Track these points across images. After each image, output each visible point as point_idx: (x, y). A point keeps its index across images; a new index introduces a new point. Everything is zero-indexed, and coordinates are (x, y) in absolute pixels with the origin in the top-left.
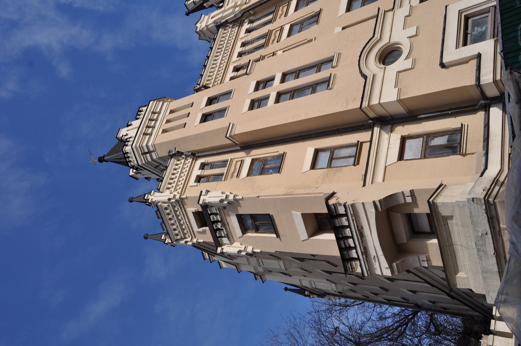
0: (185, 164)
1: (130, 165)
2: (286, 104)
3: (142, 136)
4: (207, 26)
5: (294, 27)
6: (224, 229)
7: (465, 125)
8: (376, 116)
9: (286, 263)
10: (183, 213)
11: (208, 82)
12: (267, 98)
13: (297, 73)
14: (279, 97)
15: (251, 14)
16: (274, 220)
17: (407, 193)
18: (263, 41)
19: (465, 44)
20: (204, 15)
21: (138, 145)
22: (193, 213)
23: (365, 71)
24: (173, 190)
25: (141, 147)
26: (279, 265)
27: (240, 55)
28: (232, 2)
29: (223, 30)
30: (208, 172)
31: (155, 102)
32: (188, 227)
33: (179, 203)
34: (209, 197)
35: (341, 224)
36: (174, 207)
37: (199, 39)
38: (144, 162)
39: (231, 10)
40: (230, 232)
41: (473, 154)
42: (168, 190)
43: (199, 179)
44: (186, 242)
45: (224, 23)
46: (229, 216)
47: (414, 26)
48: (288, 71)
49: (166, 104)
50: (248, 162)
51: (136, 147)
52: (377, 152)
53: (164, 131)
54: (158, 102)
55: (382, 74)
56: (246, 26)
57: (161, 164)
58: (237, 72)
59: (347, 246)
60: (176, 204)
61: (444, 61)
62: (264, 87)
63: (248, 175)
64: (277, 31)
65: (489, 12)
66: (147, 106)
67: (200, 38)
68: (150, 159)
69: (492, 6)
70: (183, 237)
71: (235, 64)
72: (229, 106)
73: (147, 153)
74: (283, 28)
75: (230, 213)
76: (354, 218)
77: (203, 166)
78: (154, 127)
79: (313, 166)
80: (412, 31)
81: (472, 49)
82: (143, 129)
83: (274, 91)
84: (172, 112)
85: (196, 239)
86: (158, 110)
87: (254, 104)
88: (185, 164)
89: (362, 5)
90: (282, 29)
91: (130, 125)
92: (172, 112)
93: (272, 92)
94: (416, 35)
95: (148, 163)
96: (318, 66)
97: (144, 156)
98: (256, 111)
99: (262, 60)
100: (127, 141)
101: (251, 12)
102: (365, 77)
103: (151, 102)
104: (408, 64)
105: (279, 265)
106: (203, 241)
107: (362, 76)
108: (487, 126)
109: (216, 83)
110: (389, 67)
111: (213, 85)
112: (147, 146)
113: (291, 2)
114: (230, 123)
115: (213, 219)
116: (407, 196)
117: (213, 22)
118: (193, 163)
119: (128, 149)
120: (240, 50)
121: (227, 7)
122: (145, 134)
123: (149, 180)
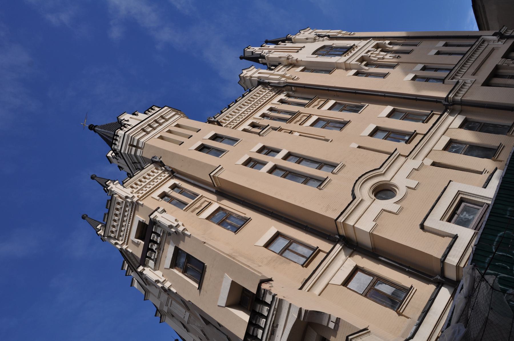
0: (160, 175)
1: (113, 147)
2: (277, 179)
3: (140, 129)
4: (251, 77)
5: (320, 121)
6: (157, 253)
7: (414, 288)
8: (344, 234)
9: (192, 316)
10: (130, 216)
11: (223, 121)
12: (264, 164)
13: (301, 159)
14: (274, 169)
15: (292, 90)
16: (205, 271)
17: (333, 319)
18: (288, 116)
19: (449, 220)
20: (254, 67)
21: (131, 135)
22: (139, 221)
23: (357, 192)
24: (135, 191)
25: (133, 139)
26: (184, 315)
27: (264, 116)
28: (283, 71)
29: (262, 88)
30: (175, 194)
31: (170, 109)
32: (127, 231)
33: (133, 205)
34: (162, 217)
35: (261, 311)
36: (126, 206)
37: (238, 83)
38: (126, 152)
39: (278, 77)
40: (160, 258)
41: (408, 318)
42: (130, 188)
43: (163, 196)
44: (116, 244)
45: (266, 83)
46: (169, 244)
47: (416, 180)
48: (295, 153)
49: (177, 116)
50: (215, 207)
51: (128, 136)
52: (328, 267)
53: (161, 138)
54: (171, 111)
55: (369, 204)
56: (282, 96)
57: (140, 163)
58: (252, 128)
59: (255, 335)
60: (130, 205)
62: (266, 154)
63: (208, 218)
64: (304, 116)
65: (482, 206)
66: (161, 108)
67: (239, 83)
68: (133, 153)
69: (487, 204)
70: (116, 238)
71: (255, 121)
72: (229, 151)
73: (134, 146)
74: (311, 117)
75: (171, 241)
76: (275, 312)
77: (174, 187)
78: (154, 129)
79: (267, 245)
80: (413, 183)
81: (453, 228)
82: (144, 125)
83: (273, 162)
84: (178, 126)
85: (127, 246)
86: (167, 117)
87: (250, 163)
88: (160, 175)
89: (385, 138)
90: (310, 116)
91: (135, 115)
92: (178, 126)
93: (271, 161)
94: (414, 189)
95: (130, 155)
96: (321, 164)
97: (130, 147)
98: (247, 169)
99: (278, 131)
100: (124, 126)
102: (354, 197)
103: (166, 108)
104: (395, 208)
105: (185, 315)
106: (132, 252)
107: (352, 195)
108: (432, 300)
109: (230, 126)
110: (378, 201)
111: (226, 126)
112: (138, 141)
113: (330, 101)
114: (220, 166)
115: (153, 237)
116: (332, 321)
117: (258, 77)
118: (168, 179)
119: (120, 133)
120: (267, 112)
121: (276, 73)
122: (143, 130)
123: (121, 170)
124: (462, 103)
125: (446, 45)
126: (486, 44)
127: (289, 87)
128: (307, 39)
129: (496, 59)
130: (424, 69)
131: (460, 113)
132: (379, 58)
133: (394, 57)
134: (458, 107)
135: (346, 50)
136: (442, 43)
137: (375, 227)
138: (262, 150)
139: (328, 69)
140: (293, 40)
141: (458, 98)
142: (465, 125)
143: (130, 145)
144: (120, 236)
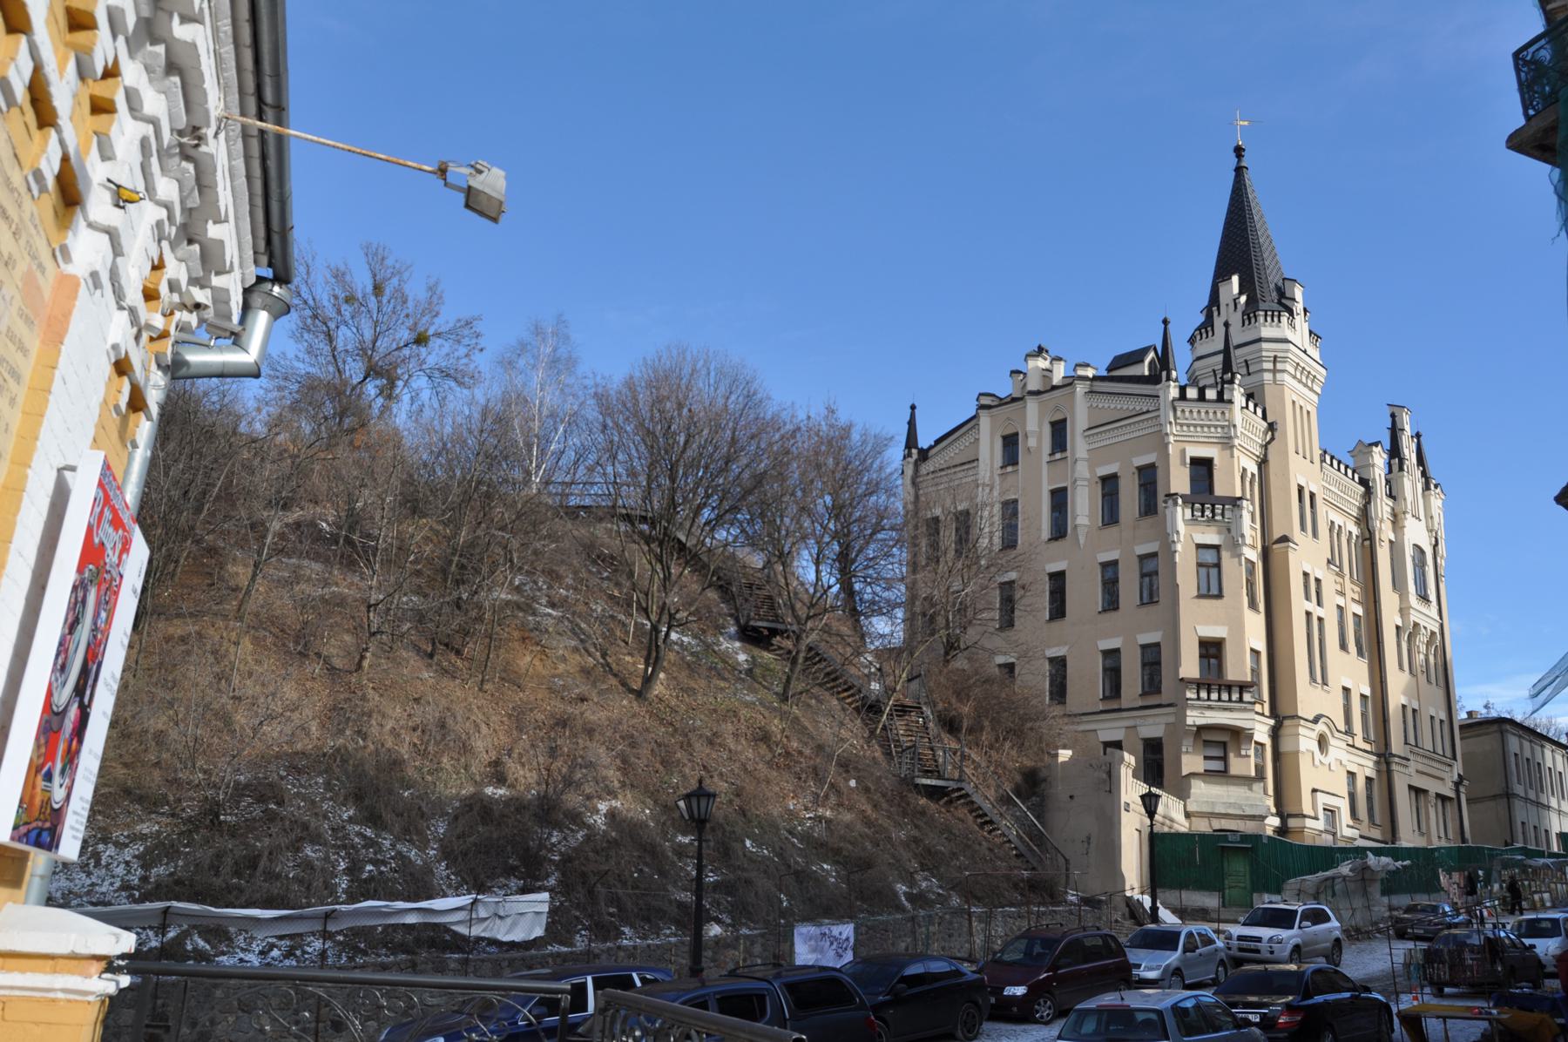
3: (1297, 361)
14: (1308, 614)
19: (1325, 809)
27: (1332, 522)
36: (1223, 427)
38: (1264, 354)
44: (1171, 423)
46: (1219, 533)
49: (1315, 398)
51: (1287, 351)
56: (1355, 531)
57: (1249, 374)
61: (1318, 793)
73: (1275, 365)
75: (1223, 537)
78: (1300, 381)
84: (1308, 412)
90: (1342, 594)
91: (1305, 314)
101: (1367, 543)
112: (1284, 371)
124: (1389, 772)
125: (1441, 721)
126: (1448, 769)
127: (1368, 536)
128: (1432, 517)
129: (1433, 787)
130: (1414, 711)
131: (1378, 771)
132: (1418, 647)
133: (1422, 666)
134: (1384, 767)
135: (1424, 598)
136: (1443, 715)
137: (1303, 753)
138: (1318, 581)
139: (1398, 584)
140: (1426, 493)
141: (1394, 767)
142: (1369, 780)
143: (1275, 357)
144: (1182, 425)
